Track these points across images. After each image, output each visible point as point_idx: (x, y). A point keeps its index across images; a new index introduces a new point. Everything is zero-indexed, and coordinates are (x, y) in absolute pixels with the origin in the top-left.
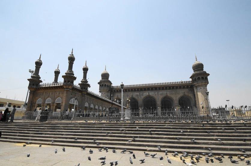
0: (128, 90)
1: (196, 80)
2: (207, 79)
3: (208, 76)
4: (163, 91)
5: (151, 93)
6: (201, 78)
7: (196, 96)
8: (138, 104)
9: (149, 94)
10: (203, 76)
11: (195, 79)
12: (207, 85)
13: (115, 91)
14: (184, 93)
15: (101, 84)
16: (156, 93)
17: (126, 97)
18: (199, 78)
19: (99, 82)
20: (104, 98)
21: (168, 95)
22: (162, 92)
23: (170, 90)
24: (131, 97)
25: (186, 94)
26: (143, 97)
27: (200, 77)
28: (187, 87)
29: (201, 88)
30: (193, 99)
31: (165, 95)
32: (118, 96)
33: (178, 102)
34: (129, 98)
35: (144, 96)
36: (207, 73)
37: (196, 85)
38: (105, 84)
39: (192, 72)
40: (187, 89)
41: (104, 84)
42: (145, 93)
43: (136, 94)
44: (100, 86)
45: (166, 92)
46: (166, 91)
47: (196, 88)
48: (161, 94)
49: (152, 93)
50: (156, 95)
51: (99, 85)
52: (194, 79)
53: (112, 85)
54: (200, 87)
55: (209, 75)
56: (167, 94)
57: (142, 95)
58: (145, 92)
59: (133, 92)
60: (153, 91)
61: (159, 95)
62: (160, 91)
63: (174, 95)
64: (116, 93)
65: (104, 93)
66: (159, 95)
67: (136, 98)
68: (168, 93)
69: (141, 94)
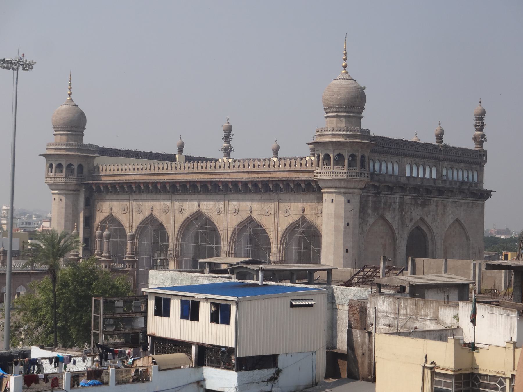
9: (199, 205)
16: (221, 204)
17: (134, 214)
21: (256, 216)
22: (235, 203)
24: (147, 215)
26: (181, 218)
32: (111, 209)
34: (141, 217)
35: (185, 216)
38: (58, 162)
48: (236, 212)
56: (251, 212)
59: (155, 196)
60: (211, 197)
63: (272, 213)
64: (108, 197)
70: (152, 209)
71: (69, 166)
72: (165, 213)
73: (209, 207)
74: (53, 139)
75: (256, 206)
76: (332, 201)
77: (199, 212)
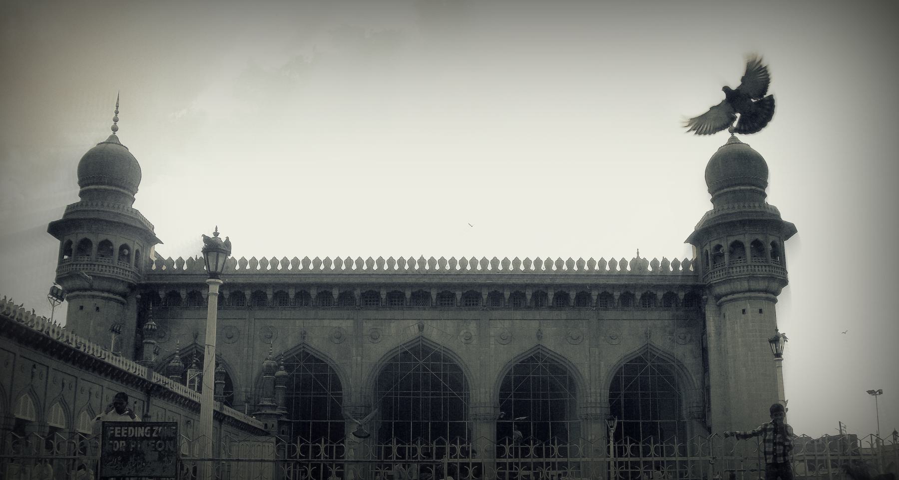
0: (276, 295)
1: (722, 255)
2: (778, 254)
3: (787, 237)
4: (518, 314)
5: (434, 323)
6: (748, 245)
7: (713, 356)
8: (340, 400)
9: (421, 328)
10: (760, 238)
11: (718, 247)
12: (777, 293)
13: (174, 296)
14: (648, 335)
15: (76, 238)
16: (473, 327)
18: (737, 246)
19: (59, 216)
20: (94, 350)
22: (507, 324)
23: (563, 314)
25: (660, 342)
27: (747, 240)
28: (670, 298)
29: (744, 311)
30: (696, 380)
31: (522, 346)
32: (196, 337)
33: (606, 393)
34: (277, 349)
36: (785, 217)
37: (719, 290)
38: (102, 237)
39: (698, 205)
40: (666, 314)
41: (95, 240)
42: (392, 325)
43: (335, 323)
44: (66, 249)
45: (535, 324)
46: (537, 314)
47: (720, 306)
49: (441, 330)
50: (469, 339)
51: (54, 245)
52: (709, 248)
53: (157, 248)
54: (742, 305)
55: (789, 230)
56: (539, 336)
57: (374, 338)
58: (397, 313)
59: (312, 313)
61: (492, 339)
62: (496, 314)
63: (587, 341)
64: (187, 313)
65: (89, 304)
66: (492, 339)
67: (331, 353)
68: (550, 330)
69: (368, 326)
70: (303, 335)
71: (124, 247)
72: (336, 341)
73: (441, 330)
74: (79, 200)
75: (550, 330)
76: (761, 311)
77: (421, 338)
